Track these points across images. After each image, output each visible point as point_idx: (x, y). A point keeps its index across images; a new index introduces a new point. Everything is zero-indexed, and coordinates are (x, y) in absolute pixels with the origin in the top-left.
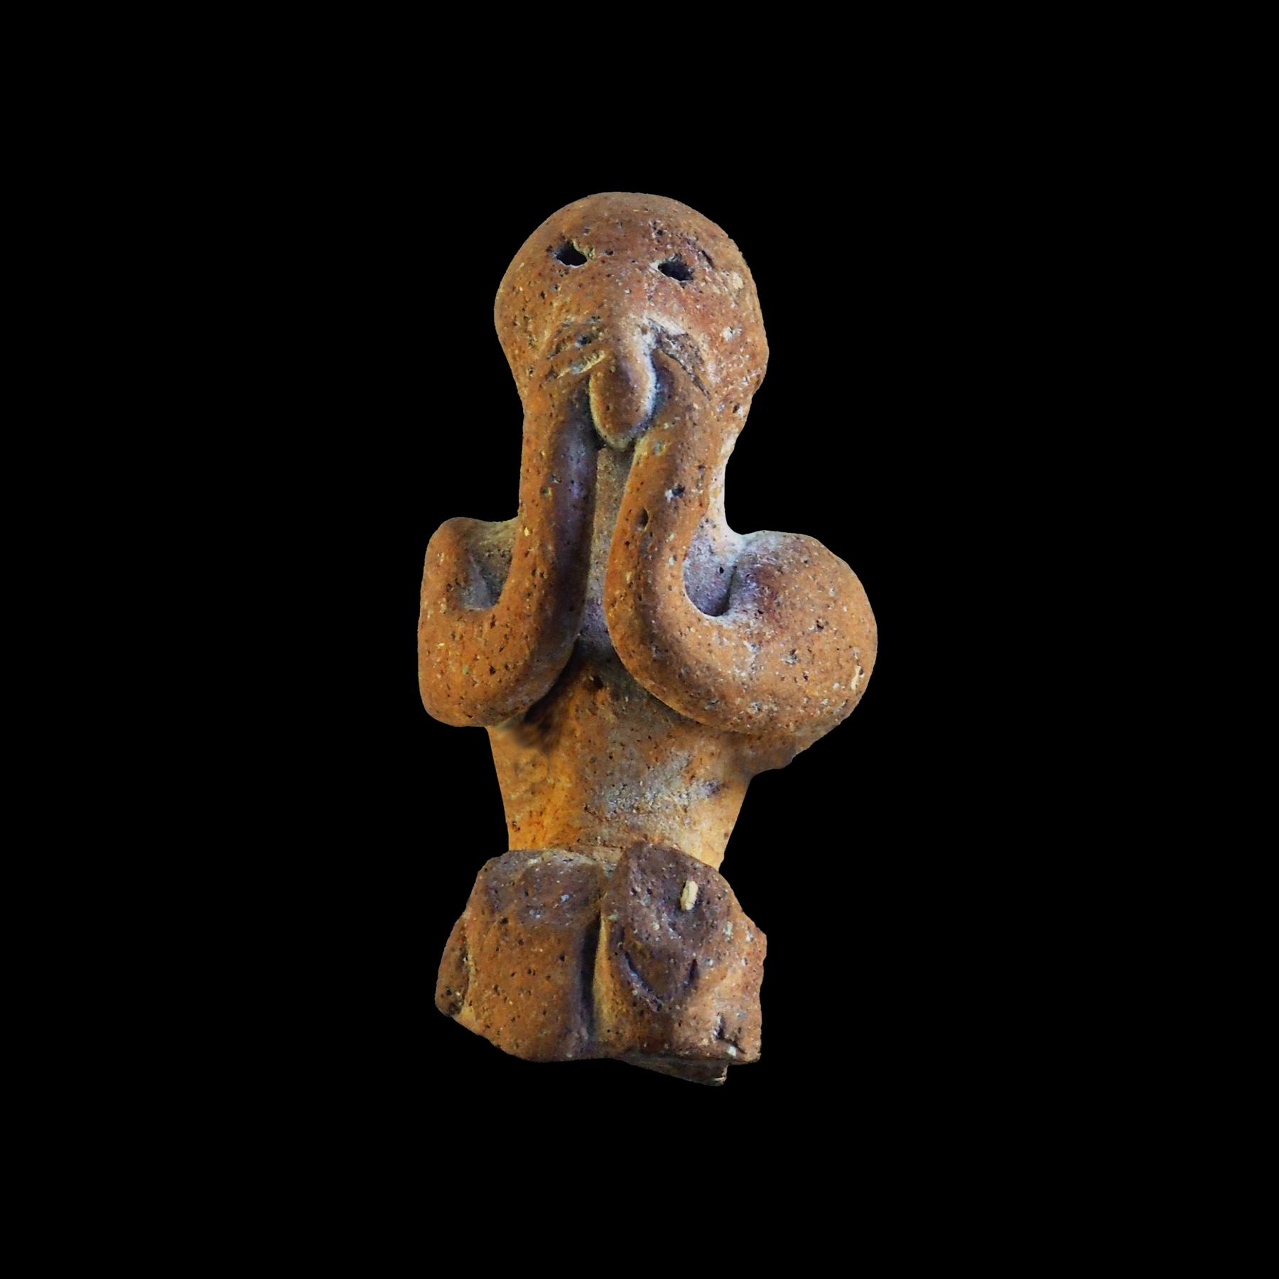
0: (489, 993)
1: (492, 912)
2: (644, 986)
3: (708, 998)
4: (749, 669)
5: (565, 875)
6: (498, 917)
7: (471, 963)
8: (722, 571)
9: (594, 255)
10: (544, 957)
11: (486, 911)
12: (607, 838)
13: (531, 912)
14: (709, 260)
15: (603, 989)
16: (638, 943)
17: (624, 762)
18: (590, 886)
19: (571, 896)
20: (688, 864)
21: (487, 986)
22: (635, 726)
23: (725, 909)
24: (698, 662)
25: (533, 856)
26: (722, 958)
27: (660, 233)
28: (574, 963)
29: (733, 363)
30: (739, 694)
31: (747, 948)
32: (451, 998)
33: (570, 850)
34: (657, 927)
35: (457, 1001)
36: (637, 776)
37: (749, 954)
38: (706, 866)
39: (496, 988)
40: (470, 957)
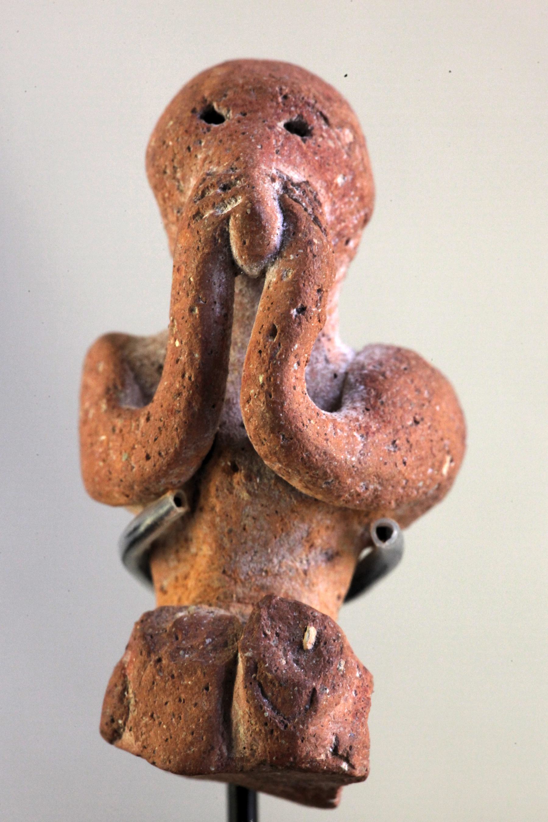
0: (146, 719)
1: (149, 653)
2: (274, 708)
3: (325, 720)
4: (358, 455)
5: (208, 623)
6: (154, 657)
7: (131, 695)
8: (335, 376)
9: (230, 115)
11: (144, 653)
13: (181, 652)
14: (326, 119)
15: (241, 713)
16: (270, 676)
18: (229, 632)
19: (213, 639)
20: (309, 613)
22: (264, 502)
23: (338, 649)
24: (317, 448)
25: (180, 609)
26: (337, 688)
27: (285, 97)
29: (345, 204)
30: (350, 475)
31: (356, 682)
32: (114, 726)
33: (210, 605)
34: (284, 662)
35: (119, 728)
36: (266, 545)
37: (358, 687)
38: (323, 615)
39: (152, 716)
40: (130, 691)
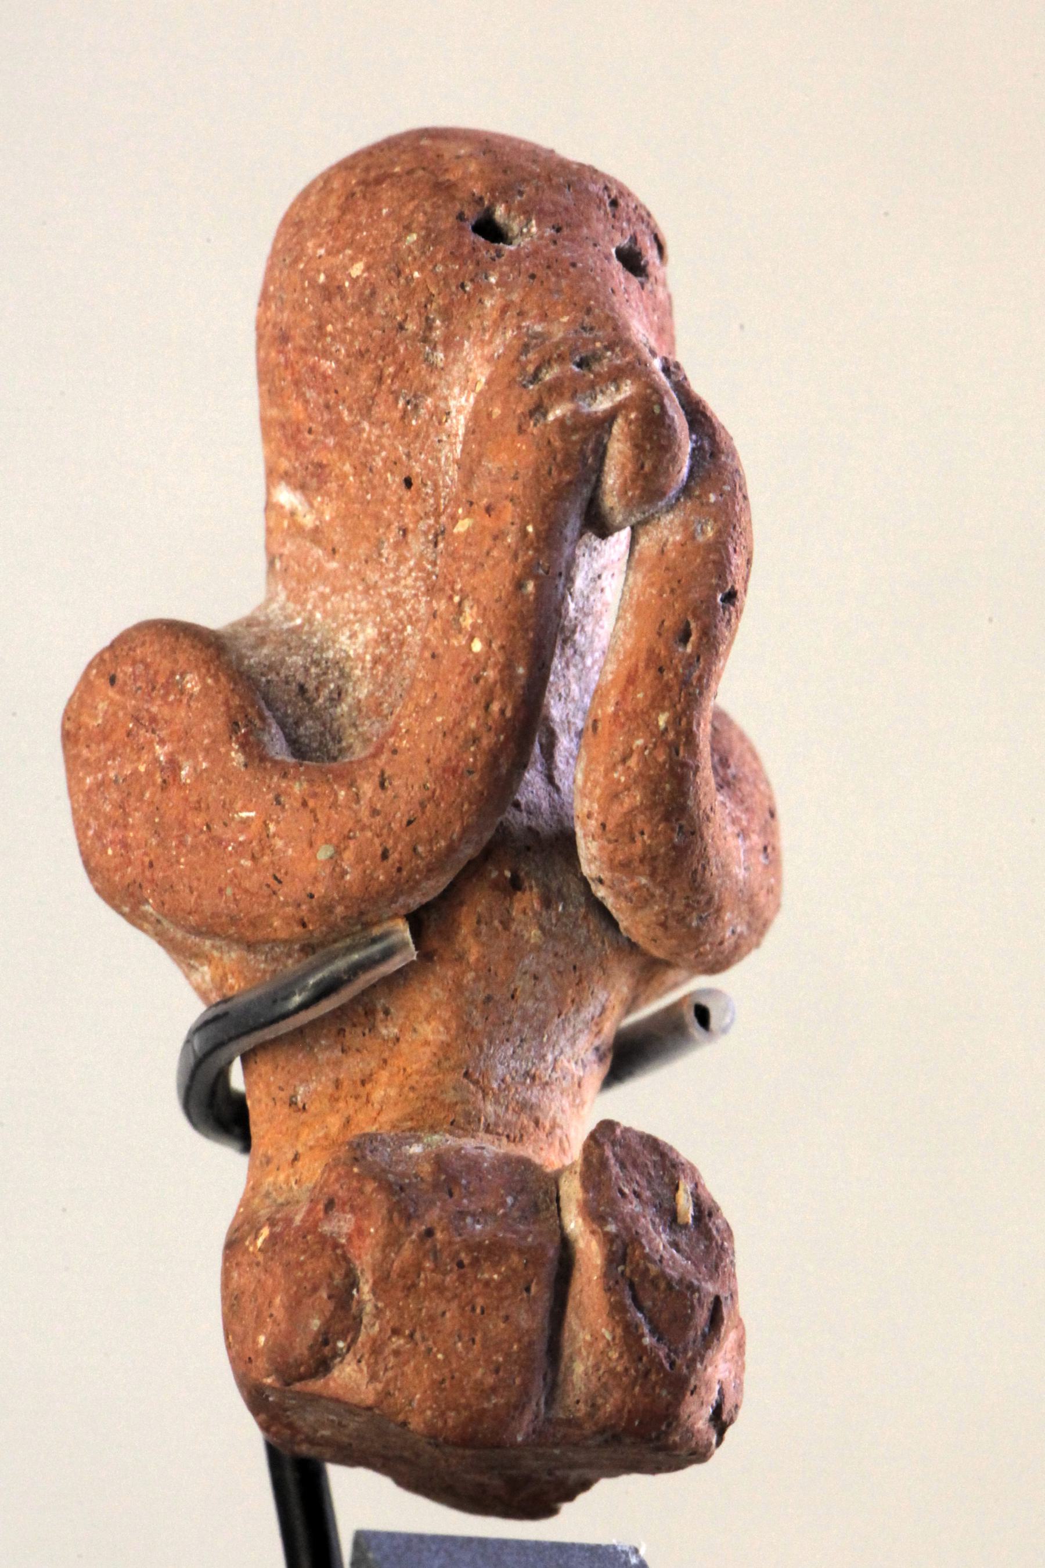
10: (499, 1287)
12: (492, 1120)
17: (530, 1004)
21: (396, 1332)
28: (547, 1296)
